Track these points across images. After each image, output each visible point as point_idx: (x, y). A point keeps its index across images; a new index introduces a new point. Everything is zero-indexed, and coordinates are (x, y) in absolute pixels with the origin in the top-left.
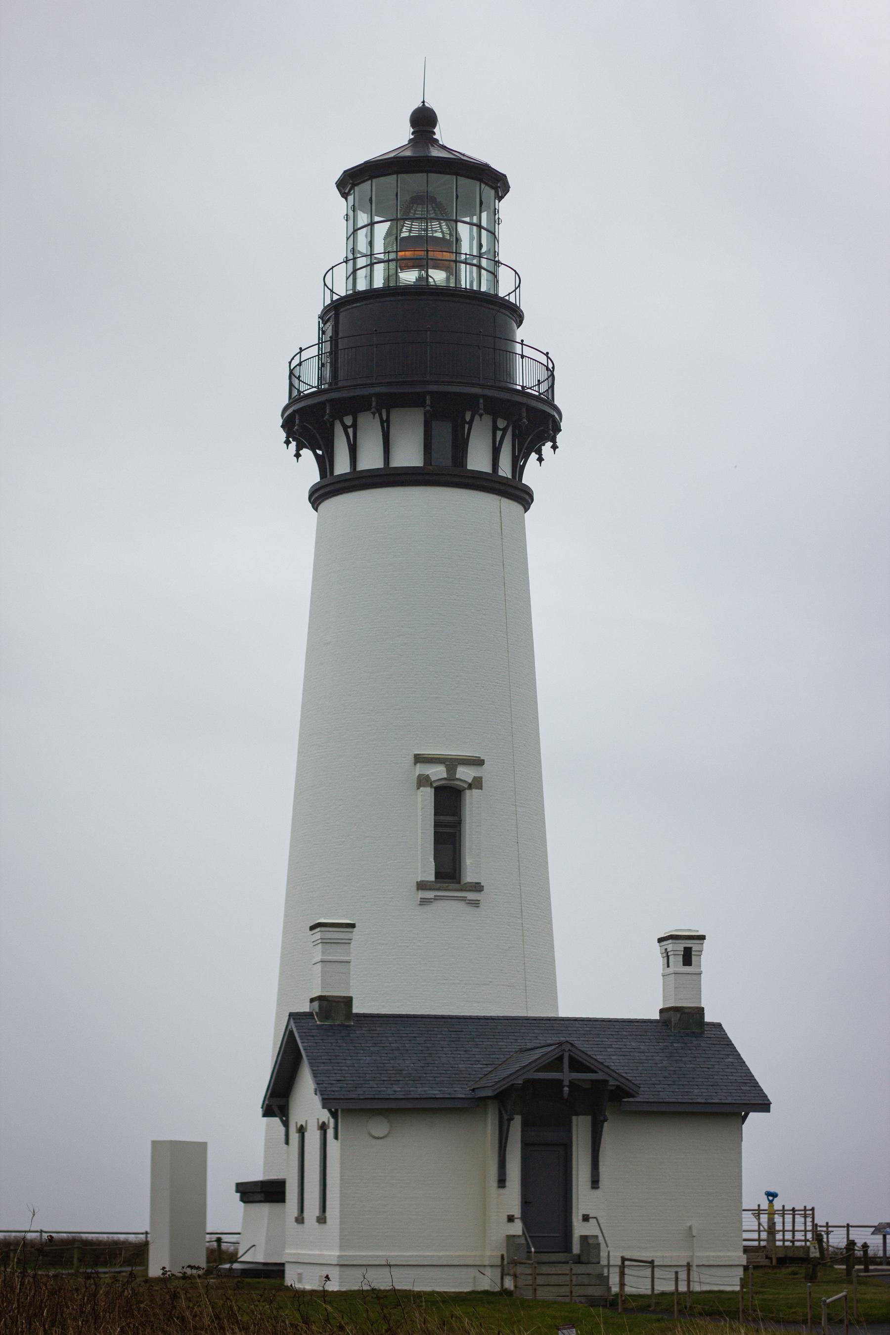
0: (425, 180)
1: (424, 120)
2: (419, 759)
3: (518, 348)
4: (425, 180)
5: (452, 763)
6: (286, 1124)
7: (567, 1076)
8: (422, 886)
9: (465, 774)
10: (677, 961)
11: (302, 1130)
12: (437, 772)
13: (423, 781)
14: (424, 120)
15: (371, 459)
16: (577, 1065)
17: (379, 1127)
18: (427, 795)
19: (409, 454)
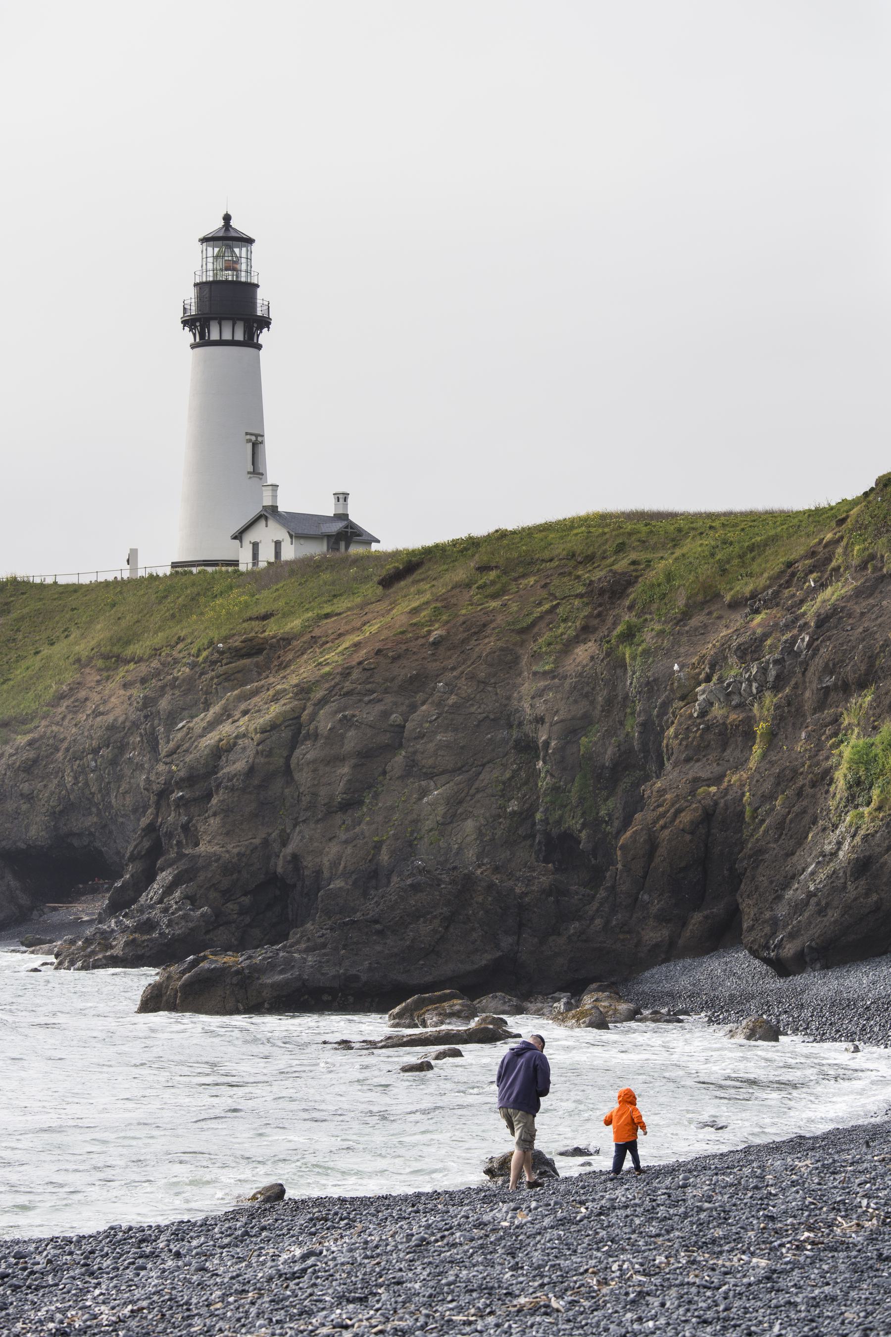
0: (228, 239)
1: (227, 218)
2: (247, 434)
3: (258, 301)
4: (228, 239)
5: (257, 436)
6: (241, 542)
7: (349, 530)
8: (249, 473)
9: (260, 439)
10: (341, 500)
11: (255, 546)
12: (253, 438)
13: (249, 441)
14: (227, 218)
15: (227, 336)
16: (351, 528)
17: (302, 541)
18: (250, 445)
19: (239, 336)
